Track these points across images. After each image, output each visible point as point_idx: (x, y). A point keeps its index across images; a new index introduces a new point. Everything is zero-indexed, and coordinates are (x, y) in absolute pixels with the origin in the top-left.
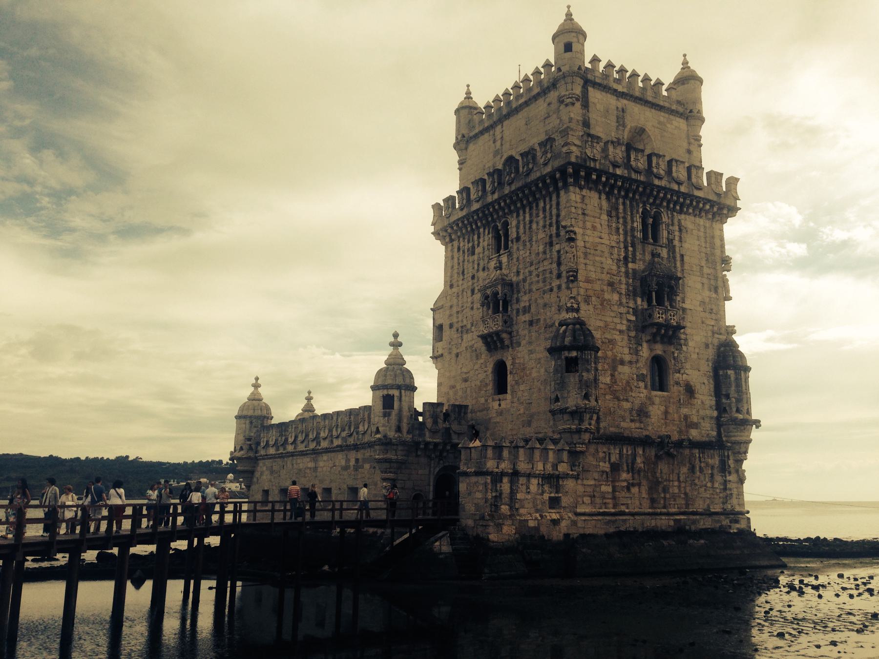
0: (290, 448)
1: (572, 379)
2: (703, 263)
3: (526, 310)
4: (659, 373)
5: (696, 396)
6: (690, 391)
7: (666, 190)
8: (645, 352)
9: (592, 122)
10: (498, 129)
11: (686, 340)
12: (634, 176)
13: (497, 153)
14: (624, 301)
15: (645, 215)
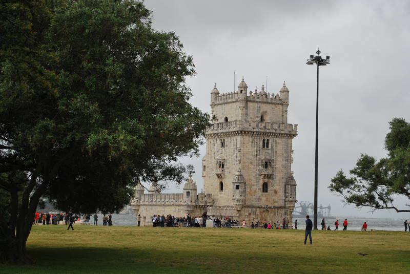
0: (154, 203)
1: (238, 191)
2: (284, 153)
3: (228, 168)
4: (265, 187)
5: (278, 193)
6: (276, 192)
7: (271, 133)
8: (261, 182)
9: (249, 113)
10: (223, 105)
11: (275, 177)
12: (260, 130)
13: (223, 114)
14: (255, 167)
15: (264, 140)
